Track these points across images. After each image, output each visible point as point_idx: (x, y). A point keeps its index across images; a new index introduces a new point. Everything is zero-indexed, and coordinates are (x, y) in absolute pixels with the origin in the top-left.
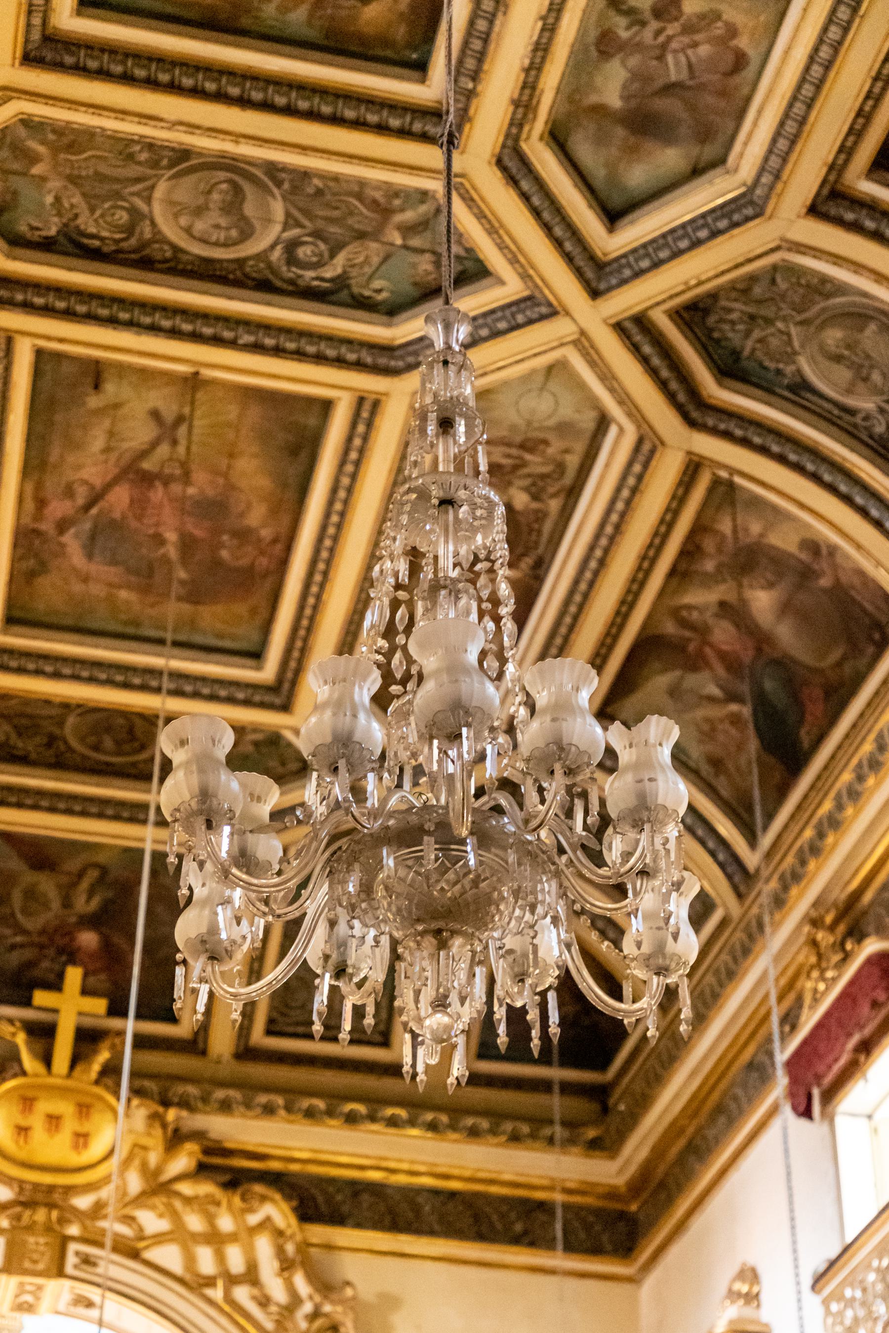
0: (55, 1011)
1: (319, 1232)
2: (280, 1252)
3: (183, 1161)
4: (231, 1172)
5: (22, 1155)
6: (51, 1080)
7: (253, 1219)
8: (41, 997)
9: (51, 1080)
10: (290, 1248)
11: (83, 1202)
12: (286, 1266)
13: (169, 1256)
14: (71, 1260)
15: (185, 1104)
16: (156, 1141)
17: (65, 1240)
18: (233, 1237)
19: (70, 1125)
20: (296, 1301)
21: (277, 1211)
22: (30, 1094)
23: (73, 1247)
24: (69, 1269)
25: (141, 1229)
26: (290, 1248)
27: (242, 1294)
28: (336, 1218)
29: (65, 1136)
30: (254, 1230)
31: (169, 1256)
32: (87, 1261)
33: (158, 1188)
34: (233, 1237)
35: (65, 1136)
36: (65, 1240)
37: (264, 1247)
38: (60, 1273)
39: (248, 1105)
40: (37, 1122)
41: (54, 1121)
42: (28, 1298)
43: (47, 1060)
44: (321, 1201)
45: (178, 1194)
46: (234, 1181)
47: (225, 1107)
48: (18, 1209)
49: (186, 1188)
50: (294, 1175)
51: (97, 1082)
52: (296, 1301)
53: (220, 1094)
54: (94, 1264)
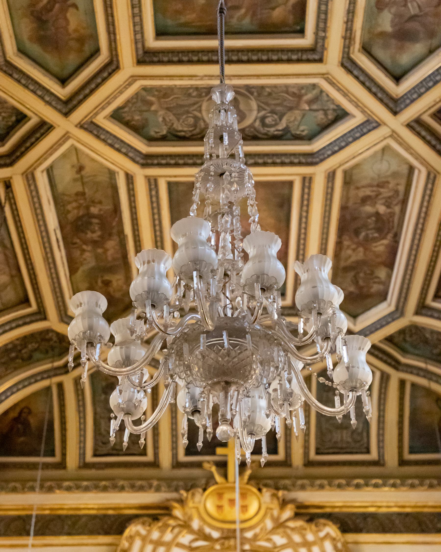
0: (226, 456)
1: (351, 537)
3: (288, 513)
4: (309, 515)
5: (221, 517)
6: (228, 485)
7: (322, 534)
8: (219, 451)
9: (228, 485)
11: (249, 535)
15: (285, 488)
16: (275, 505)
21: (331, 530)
22: (221, 491)
26: (339, 545)
28: (358, 530)
33: (280, 525)
39: (312, 485)
43: (225, 476)
44: (350, 523)
45: (288, 527)
46: (311, 519)
47: (303, 488)
48: (222, 541)
49: (291, 524)
51: (248, 483)
53: (300, 482)
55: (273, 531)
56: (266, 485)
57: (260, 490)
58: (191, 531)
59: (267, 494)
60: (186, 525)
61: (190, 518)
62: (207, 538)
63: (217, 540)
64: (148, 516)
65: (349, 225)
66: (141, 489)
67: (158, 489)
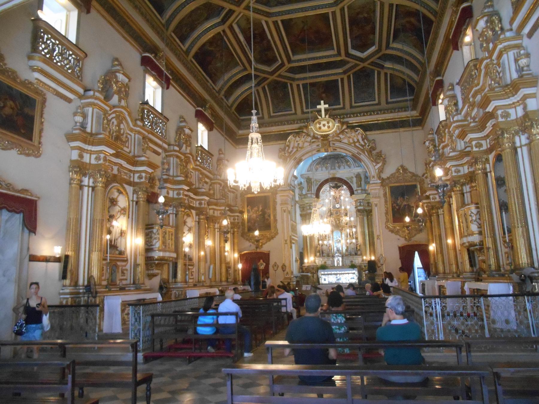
1: (368, 133)
2: (362, 137)
3: (345, 127)
4: (352, 127)
11: (331, 136)
12: (363, 140)
19: (327, 125)
20: (366, 144)
21: (360, 131)
27: (357, 144)
28: (370, 130)
29: (326, 127)
31: (346, 141)
33: (342, 132)
36: (330, 141)
40: (321, 125)
41: (324, 125)
43: (321, 116)
44: (367, 128)
49: (346, 130)
52: (366, 144)
55: (340, 134)
57: (334, 120)
59: (337, 121)
60: (308, 135)
64: (295, 132)
65: (354, 22)
66: (291, 124)
67: (297, 123)
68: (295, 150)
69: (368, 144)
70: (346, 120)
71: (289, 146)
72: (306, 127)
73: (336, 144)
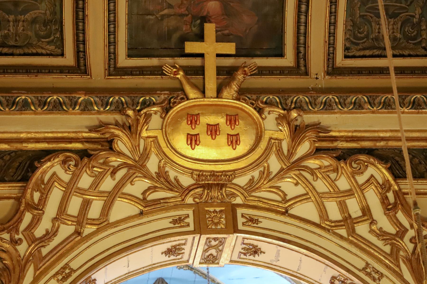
0: (202, 55)
2: (384, 200)
3: (304, 148)
6: (206, 101)
7: (361, 179)
8: (191, 47)
9: (206, 101)
10: (391, 196)
13: (308, 210)
14: (240, 220)
15: (299, 107)
17: (234, 208)
18: (349, 193)
23: (240, 211)
24: (240, 227)
25: (285, 195)
26: (391, 196)
30: (362, 188)
31: (308, 210)
32: (252, 220)
34: (349, 193)
35: (222, 139)
36: (234, 208)
37: (373, 198)
38: (236, 230)
39: (343, 104)
42: (213, 252)
45: (306, 168)
46: (344, 156)
47: (328, 107)
48: (199, 190)
50: (382, 149)
53: (323, 98)
54: (257, 221)
55: (282, 174)
56: (268, 103)
58: (147, 175)
61: (145, 156)
62: (172, 185)
63: (189, 189)
68: (66, 230)
69: (411, 233)
70: (310, 118)
71: (38, 208)
72: (131, 129)
73: (265, 223)
